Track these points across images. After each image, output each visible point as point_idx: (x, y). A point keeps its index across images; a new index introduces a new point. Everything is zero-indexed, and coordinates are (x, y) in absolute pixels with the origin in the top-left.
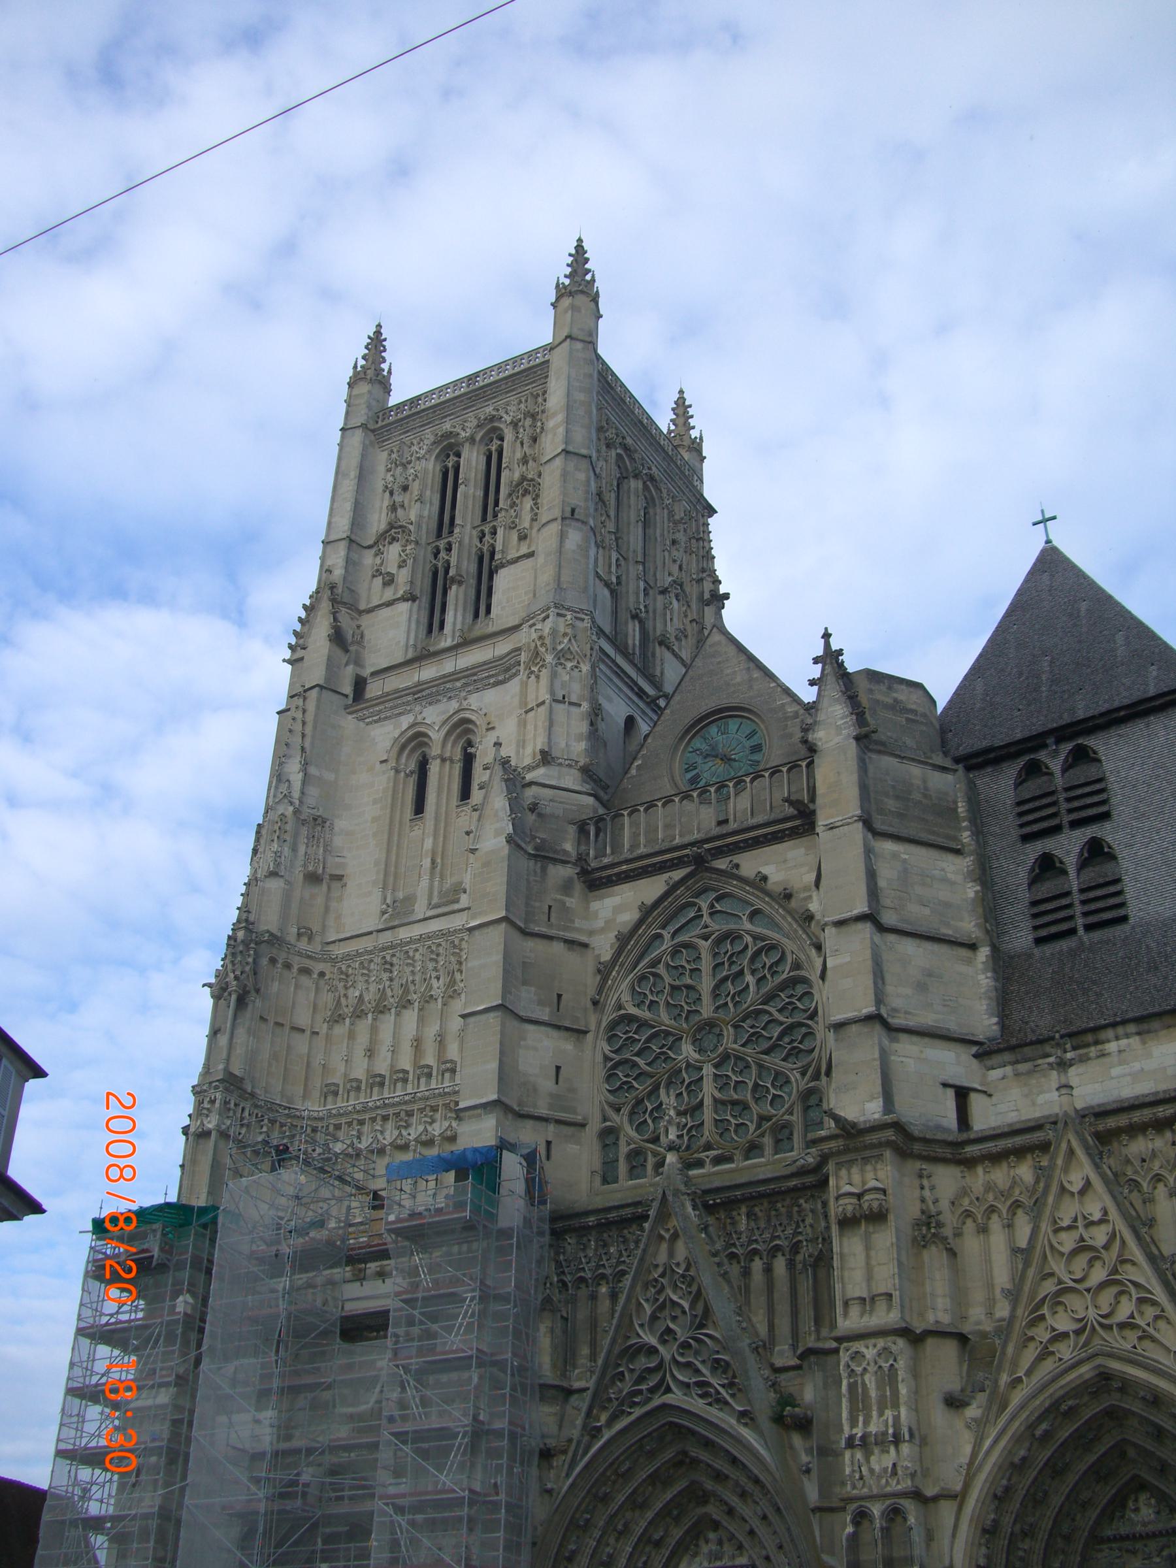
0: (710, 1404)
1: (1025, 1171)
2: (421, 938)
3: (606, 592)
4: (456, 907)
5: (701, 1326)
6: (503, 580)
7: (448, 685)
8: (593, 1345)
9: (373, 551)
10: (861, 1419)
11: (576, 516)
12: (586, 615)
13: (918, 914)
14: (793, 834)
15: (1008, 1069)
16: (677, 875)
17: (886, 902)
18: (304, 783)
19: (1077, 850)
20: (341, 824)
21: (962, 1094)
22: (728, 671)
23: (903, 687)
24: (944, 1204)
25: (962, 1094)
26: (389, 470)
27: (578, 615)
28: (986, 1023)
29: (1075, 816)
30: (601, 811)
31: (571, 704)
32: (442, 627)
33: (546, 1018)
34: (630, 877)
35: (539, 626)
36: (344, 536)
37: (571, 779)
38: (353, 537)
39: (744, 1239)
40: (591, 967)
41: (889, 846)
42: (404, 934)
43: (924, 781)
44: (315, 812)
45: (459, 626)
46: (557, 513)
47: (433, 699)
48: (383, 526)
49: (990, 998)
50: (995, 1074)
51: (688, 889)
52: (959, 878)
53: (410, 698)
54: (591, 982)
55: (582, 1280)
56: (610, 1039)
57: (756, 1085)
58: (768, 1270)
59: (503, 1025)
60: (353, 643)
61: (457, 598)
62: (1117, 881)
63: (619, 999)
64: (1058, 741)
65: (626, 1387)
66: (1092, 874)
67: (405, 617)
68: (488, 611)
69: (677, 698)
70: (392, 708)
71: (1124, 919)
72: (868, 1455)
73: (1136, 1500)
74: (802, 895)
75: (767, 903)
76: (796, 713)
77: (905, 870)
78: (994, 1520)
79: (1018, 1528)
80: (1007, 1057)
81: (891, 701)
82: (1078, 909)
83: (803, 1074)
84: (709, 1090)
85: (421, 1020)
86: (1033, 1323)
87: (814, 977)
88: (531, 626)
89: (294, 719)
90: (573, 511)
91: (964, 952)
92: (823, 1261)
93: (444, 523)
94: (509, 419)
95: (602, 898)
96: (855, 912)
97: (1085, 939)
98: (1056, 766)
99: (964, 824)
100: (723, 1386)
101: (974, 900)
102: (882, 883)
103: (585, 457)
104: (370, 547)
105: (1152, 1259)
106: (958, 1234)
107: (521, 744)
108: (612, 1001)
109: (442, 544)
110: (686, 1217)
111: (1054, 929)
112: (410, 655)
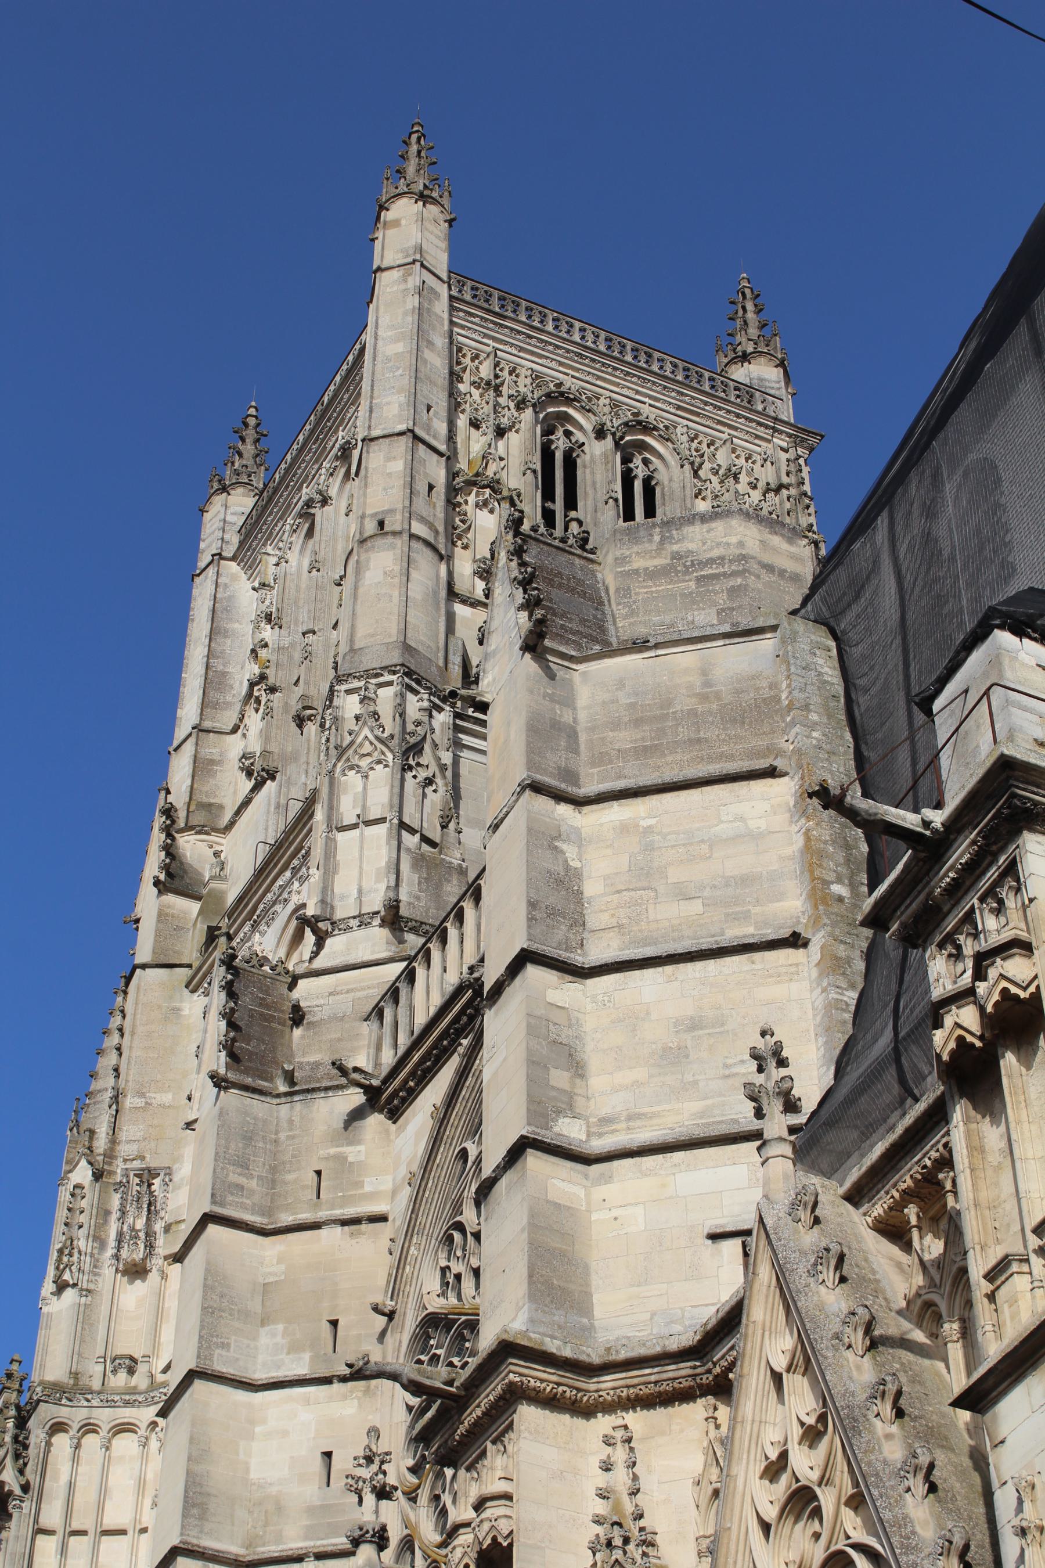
7: (280, 882)
11: (387, 529)
12: (394, 673)
27: (381, 679)
31: (369, 823)
34: (429, 1070)
38: (207, 724)
44: (137, 1164)
77: (649, 848)
81: (668, 561)
90: (381, 524)
102: (591, 888)
103: (401, 434)
104: (235, 730)
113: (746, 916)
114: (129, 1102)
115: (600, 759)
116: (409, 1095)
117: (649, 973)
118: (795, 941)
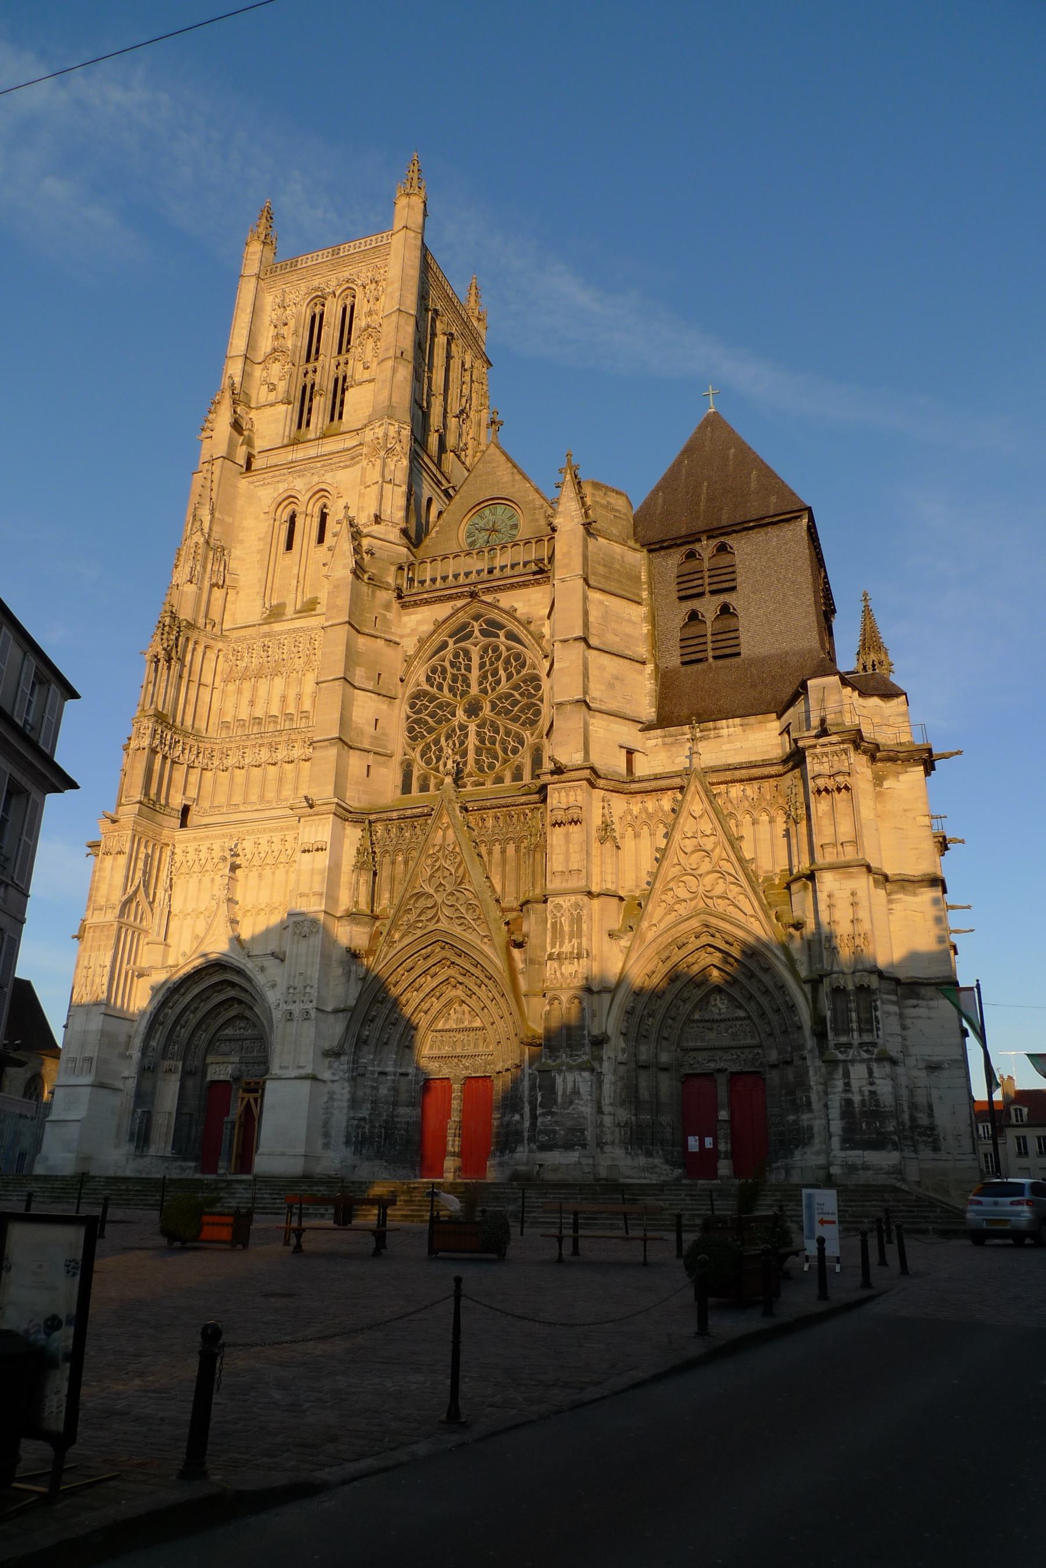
0: (465, 930)
1: (666, 802)
2: (289, 631)
3: (420, 413)
4: (313, 613)
5: (461, 883)
6: (351, 396)
7: (311, 465)
8: (392, 892)
9: (261, 367)
10: (558, 944)
13: (612, 640)
14: (537, 583)
15: (660, 740)
16: (460, 603)
17: (592, 630)
18: (211, 522)
19: (713, 609)
20: (236, 552)
21: (630, 752)
22: (499, 473)
23: (614, 494)
24: (615, 819)
25: (630, 752)
26: (274, 310)
28: (648, 711)
29: (714, 587)
30: (412, 558)
31: (394, 484)
32: (308, 424)
33: (371, 688)
35: (376, 431)
36: (242, 353)
37: (394, 535)
39: (490, 831)
40: (401, 658)
41: (595, 596)
42: (277, 627)
43: (622, 557)
45: (320, 426)
46: (391, 353)
47: (301, 474)
48: (269, 350)
49: (651, 696)
50: (652, 742)
51: (466, 613)
52: (639, 620)
53: (285, 471)
54: (400, 668)
55: (387, 851)
56: (412, 706)
57: (502, 738)
58: (503, 852)
59: (344, 690)
60: (246, 430)
61: (321, 404)
62: (737, 630)
63: (417, 679)
64: (709, 538)
65: (412, 917)
66: (719, 625)
67: (283, 415)
68: (340, 417)
69: (464, 488)
70: (273, 477)
71: (739, 654)
72: (561, 965)
73: (716, 1000)
74: (539, 623)
75: (516, 626)
76: (542, 505)
77: (607, 612)
78: (633, 1007)
79: (645, 1012)
80: (659, 732)
82: (710, 645)
83: (532, 735)
84: (472, 741)
85: (287, 684)
86: (664, 892)
87: (543, 674)
88: (371, 430)
89: (205, 478)
90: (402, 353)
91: (638, 665)
92: (540, 848)
93: (312, 353)
94: (360, 283)
95: (409, 614)
96: (574, 635)
97: (713, 665)
98: (706, 554)
99: (645, 586)
100: (473, 920)
101: (646, 634)
102: (591, 619)
105: (741, 860)
106: (623, 837)
107: (361, 509)
108: (413, 681)
109: (310, 367)
110: (455, 817)
111: (694, 657)
112: (286, 441)
113: (629, 649)
114: (217, 515)
115: (595, 574)
116: (416, 604)
117: (606, 655)
118: (644, 663)
